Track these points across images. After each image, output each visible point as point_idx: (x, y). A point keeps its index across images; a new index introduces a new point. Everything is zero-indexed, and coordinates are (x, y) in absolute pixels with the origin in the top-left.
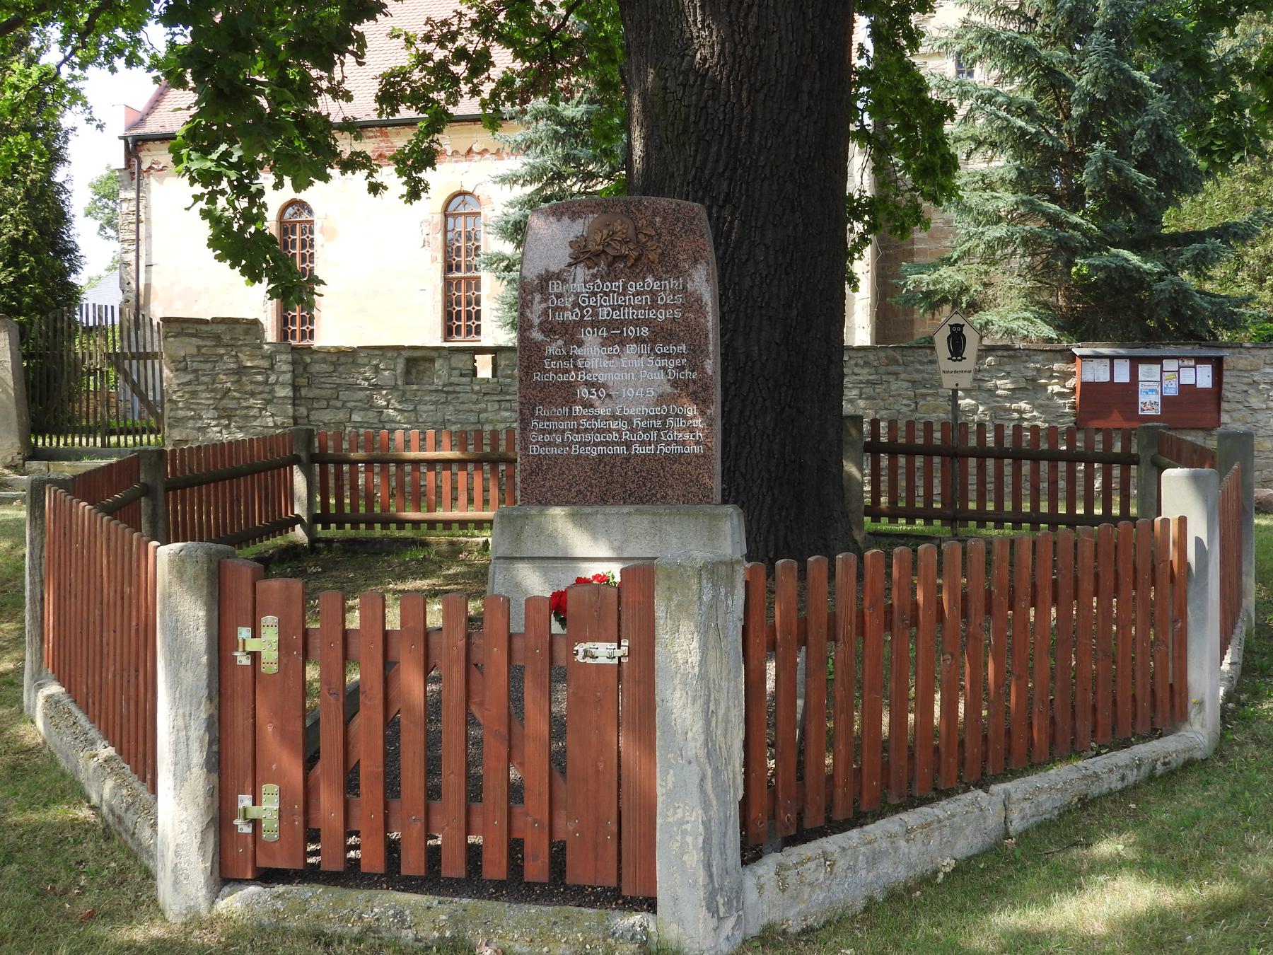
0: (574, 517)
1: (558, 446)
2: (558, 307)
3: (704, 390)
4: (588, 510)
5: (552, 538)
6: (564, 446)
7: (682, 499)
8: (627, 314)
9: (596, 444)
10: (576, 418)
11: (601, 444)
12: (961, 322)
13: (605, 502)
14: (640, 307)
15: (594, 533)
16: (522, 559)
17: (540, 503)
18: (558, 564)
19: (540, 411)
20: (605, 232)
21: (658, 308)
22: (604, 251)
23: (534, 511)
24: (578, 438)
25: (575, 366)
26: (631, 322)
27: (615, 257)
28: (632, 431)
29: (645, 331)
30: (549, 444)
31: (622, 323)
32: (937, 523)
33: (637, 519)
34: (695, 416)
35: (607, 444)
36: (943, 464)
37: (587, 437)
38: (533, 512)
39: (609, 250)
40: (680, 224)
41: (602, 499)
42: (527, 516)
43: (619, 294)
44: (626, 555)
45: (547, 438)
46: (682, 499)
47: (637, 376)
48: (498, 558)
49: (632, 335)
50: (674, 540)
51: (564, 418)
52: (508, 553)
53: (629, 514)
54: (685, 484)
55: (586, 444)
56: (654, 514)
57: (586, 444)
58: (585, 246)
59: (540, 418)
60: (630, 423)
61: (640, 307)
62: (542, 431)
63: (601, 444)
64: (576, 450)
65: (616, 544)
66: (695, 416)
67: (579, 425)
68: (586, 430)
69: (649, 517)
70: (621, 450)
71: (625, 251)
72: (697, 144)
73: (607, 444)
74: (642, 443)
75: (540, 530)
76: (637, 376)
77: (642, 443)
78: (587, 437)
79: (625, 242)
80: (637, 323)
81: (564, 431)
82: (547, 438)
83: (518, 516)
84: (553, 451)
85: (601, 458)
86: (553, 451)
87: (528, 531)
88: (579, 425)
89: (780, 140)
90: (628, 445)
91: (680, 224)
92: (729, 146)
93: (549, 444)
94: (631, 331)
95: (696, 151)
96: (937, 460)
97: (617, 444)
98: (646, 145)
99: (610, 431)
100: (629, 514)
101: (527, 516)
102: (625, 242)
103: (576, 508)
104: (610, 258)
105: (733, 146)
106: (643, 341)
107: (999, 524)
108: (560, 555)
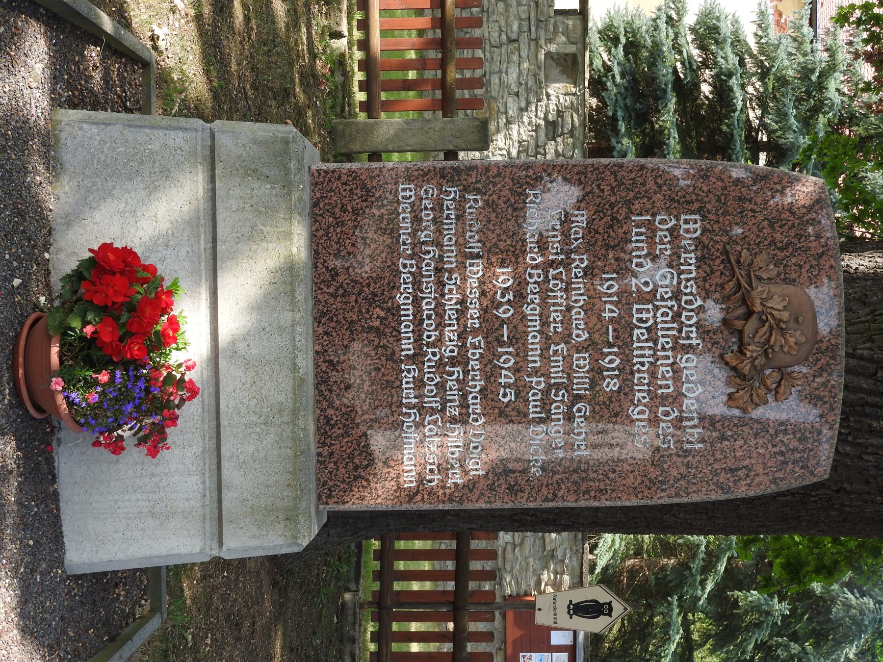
0: (289, 269)
1: (413, 234)
2: (654, 231)
3: (510, 488)
4: (303, 293)
5: (251, 236)
6: (414, 245)
7: (325, 451)
8: (641, 350)
9: (417, 302)
10: (462, 266)
11: (418, 310)
12: (615, 614)
13: (318, 320)
14: (653, 375)
15: (262, 306)
16: (212, 179)
17: (315, 205)
18: (204, 244)
19: (475, 202)
20: (785, 315)
21: (652, 409)
22: (749, 314)
23: (302, 192)
24: (428, 269)
25: (552, 264)
26: (627, 360)
27: (740, 333)
28: (440, 364)
29: (611, 385)
30: (417, 219)
31: (625, 345)
32: (376, 586)
33: (286, 383)
34: (466, 472)
35: (418, 322)
36: (444, 593)
37: (429, 284)
38: (295, 196)
39: (753, 323)
40: (794, 444)
41: (323, 314)
42: (288, 186)
43: (676, 339)
44: (222, 364)
45: (427, 216)
46: (325, 451)
47: (536, 372)
48: (213, 136)
49: (605, 363)
50: (250, 449)
51: (461, 245)
52: (221, 152)
53: (295, 368)
54: (351, 457)
55: (417, 284)
56: (295, 412)
57: (417, 284)
58: (760, 279)
59: (461, 203)
60: (453, 361)
61: (653, 375)
62: (439, 206)
63: (418, 310)
64: (406, 267)
65: (242, 347)
66: (466, 472)
67: (450, 271)
68: (441, 284)
69: (289, 404)
70: (408, 346)
71: (752, 350)
72: (871, 360)
73: (418, 322)
74: (419, 383)
75: (266, 211)
76: (536, 372)
77: (419, 383)
78: (429, 284)
79: (767, 348)
80: (626, 371)
81: (439, 245)
82: (427, 216)
83: (287, 172)
84: (406, 226)
85: (395, 311)
86: (406, 226)
87: (262, 190)
88: (450, 271)
89: (873, 472)
90: (417, 358)
91: (794, 444)
92: (867, 404)
93: (417, 219)
94: (612, 361)
95: (861, 358)
96: (450, 586)
97: (418, 339)
98: (865, 276)
99: (440, 326)
100: (295, 368)
101: (288, 186)
102: (767, 348)
103: (305, 273)
104: (739, 324)
105: (868, 410)
106: (593, 384)
107: (376, 637)
108: (221, 247)
